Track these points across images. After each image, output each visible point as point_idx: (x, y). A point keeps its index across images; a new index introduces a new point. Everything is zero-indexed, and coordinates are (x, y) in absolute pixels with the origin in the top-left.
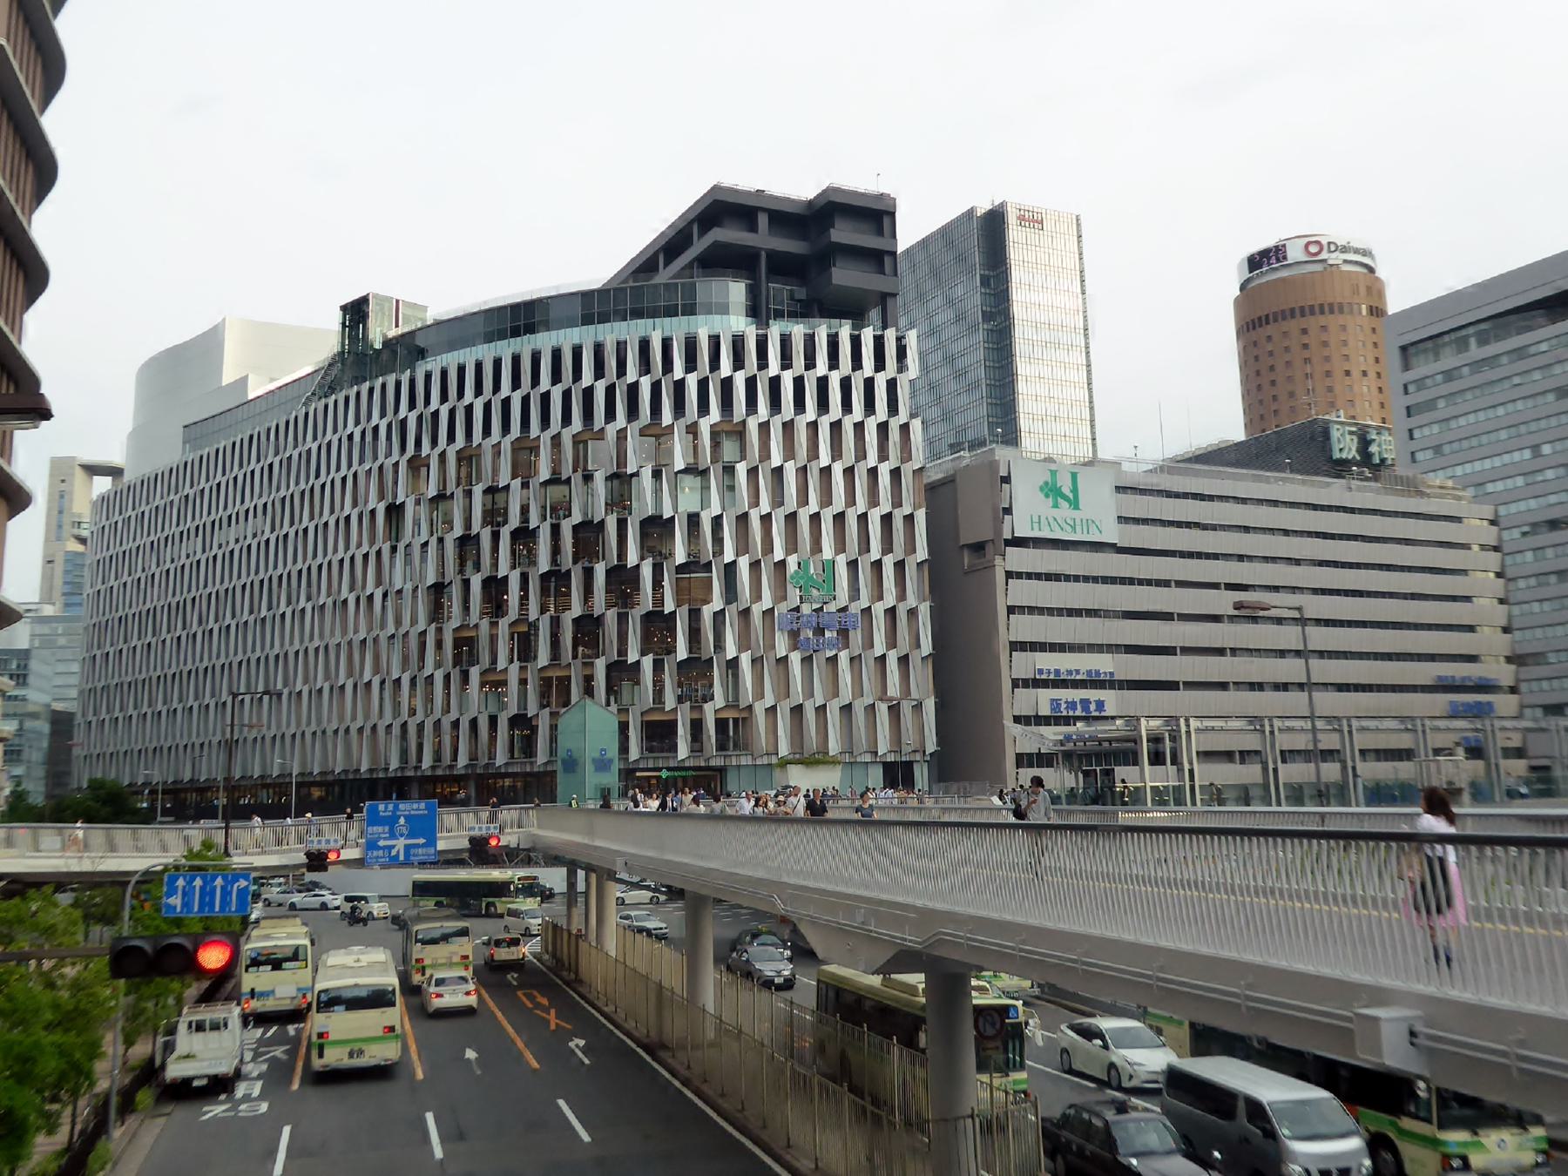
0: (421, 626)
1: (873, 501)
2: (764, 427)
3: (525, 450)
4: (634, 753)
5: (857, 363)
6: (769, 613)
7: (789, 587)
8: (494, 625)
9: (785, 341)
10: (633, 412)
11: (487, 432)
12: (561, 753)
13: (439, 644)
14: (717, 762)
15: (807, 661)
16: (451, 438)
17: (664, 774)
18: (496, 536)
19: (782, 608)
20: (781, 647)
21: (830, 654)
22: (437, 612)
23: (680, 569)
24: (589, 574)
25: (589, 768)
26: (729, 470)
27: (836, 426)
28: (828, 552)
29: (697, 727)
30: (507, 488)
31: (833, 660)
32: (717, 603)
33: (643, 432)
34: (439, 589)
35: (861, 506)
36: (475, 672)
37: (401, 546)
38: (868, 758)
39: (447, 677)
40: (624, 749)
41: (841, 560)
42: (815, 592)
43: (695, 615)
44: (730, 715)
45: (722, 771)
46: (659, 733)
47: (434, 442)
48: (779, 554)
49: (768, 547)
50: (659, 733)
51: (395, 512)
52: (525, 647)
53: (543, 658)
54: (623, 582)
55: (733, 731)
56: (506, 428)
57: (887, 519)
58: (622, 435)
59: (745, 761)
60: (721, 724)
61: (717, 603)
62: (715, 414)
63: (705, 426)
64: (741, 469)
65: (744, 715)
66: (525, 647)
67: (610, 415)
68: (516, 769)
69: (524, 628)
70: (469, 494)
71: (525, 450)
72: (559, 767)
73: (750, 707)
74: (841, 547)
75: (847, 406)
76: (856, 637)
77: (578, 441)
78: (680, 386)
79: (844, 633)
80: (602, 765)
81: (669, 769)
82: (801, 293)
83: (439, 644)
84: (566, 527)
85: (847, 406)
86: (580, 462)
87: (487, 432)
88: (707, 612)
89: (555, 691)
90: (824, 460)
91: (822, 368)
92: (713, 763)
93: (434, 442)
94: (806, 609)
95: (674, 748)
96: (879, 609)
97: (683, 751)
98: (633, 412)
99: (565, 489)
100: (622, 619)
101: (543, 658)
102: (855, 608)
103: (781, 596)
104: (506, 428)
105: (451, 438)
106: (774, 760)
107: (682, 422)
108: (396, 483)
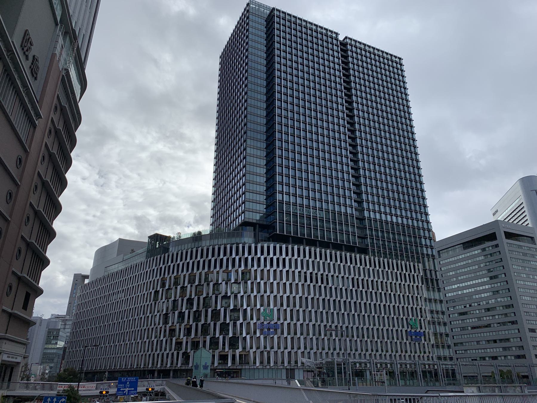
0: (161, 325)
1: (285, 292)
5: (281, 254)
8: (180, 325)
9: (262, 248)
10: (221, 266)
11: (182, 271)
12: (195, 364)
13: (165, 331)
15: (265, 338)
16: (173, 273)
17: (224, 371)
18: (183, 300)
19: (259, 322)
21: (271, 336)
22: (166, 322)
23: (231, 310)
24: (207, 311)
26: (246, 283)
27: (275, 271)
28: (272, 306)
29: (234, 357)
30: (187, 286)
32: (241, 320)
33: (223, 272)
34: (166, 315)
36: (174, 339)
37: (157, 302)
39: (166, 341)
40: (213, 363)
41: (275, 309)
42: (268, 318)
44: (243, 353)
45: (241, 369)
46: (223, 358)
47: (169, 274)
48: (258, 307)
49: (255, 305)
50: (223, 358)
51: (157, 292)
52: (188, 331)
53: (193, 335)
54: (216, 314)
55: (244, 359)
56: (188, 270)
58: (218, 273)
59: (247, 367)
60: (240, 355)
61: (241, 320)
62: (243, 267)
63: (240, 270)
65: (247, 353)
66: (188, 331)
67: (215, 267)
68: (184, 368)
69: (189, 327)
70: (176, 288)
72: (193, 368)
75: (278, 266)
76: (279, 331)
77: (206, 274)
78: (234, 259)
79: (276, 330)
80: (205, 367)
81: (226, 369)
82: (267, 235)
83: (165, 331)
84: (201, 298)
85: (278, 266)
86: (206, 279)
87: (182, 271)
88: (238, 323)
89: (195, 345)
90: (271, 281)
92: (238, 368)
93: (169, 274)
94: (265, 323)
96: (286, 323)
97: (230, 364)
98: (221, 266)
99: (201, 287)
101: (193, 335)
102: (279, 323)
103: (258, 319)
104: (188, 270)
105: (173, 273)
107: (234, 269)
108: (157, 285)
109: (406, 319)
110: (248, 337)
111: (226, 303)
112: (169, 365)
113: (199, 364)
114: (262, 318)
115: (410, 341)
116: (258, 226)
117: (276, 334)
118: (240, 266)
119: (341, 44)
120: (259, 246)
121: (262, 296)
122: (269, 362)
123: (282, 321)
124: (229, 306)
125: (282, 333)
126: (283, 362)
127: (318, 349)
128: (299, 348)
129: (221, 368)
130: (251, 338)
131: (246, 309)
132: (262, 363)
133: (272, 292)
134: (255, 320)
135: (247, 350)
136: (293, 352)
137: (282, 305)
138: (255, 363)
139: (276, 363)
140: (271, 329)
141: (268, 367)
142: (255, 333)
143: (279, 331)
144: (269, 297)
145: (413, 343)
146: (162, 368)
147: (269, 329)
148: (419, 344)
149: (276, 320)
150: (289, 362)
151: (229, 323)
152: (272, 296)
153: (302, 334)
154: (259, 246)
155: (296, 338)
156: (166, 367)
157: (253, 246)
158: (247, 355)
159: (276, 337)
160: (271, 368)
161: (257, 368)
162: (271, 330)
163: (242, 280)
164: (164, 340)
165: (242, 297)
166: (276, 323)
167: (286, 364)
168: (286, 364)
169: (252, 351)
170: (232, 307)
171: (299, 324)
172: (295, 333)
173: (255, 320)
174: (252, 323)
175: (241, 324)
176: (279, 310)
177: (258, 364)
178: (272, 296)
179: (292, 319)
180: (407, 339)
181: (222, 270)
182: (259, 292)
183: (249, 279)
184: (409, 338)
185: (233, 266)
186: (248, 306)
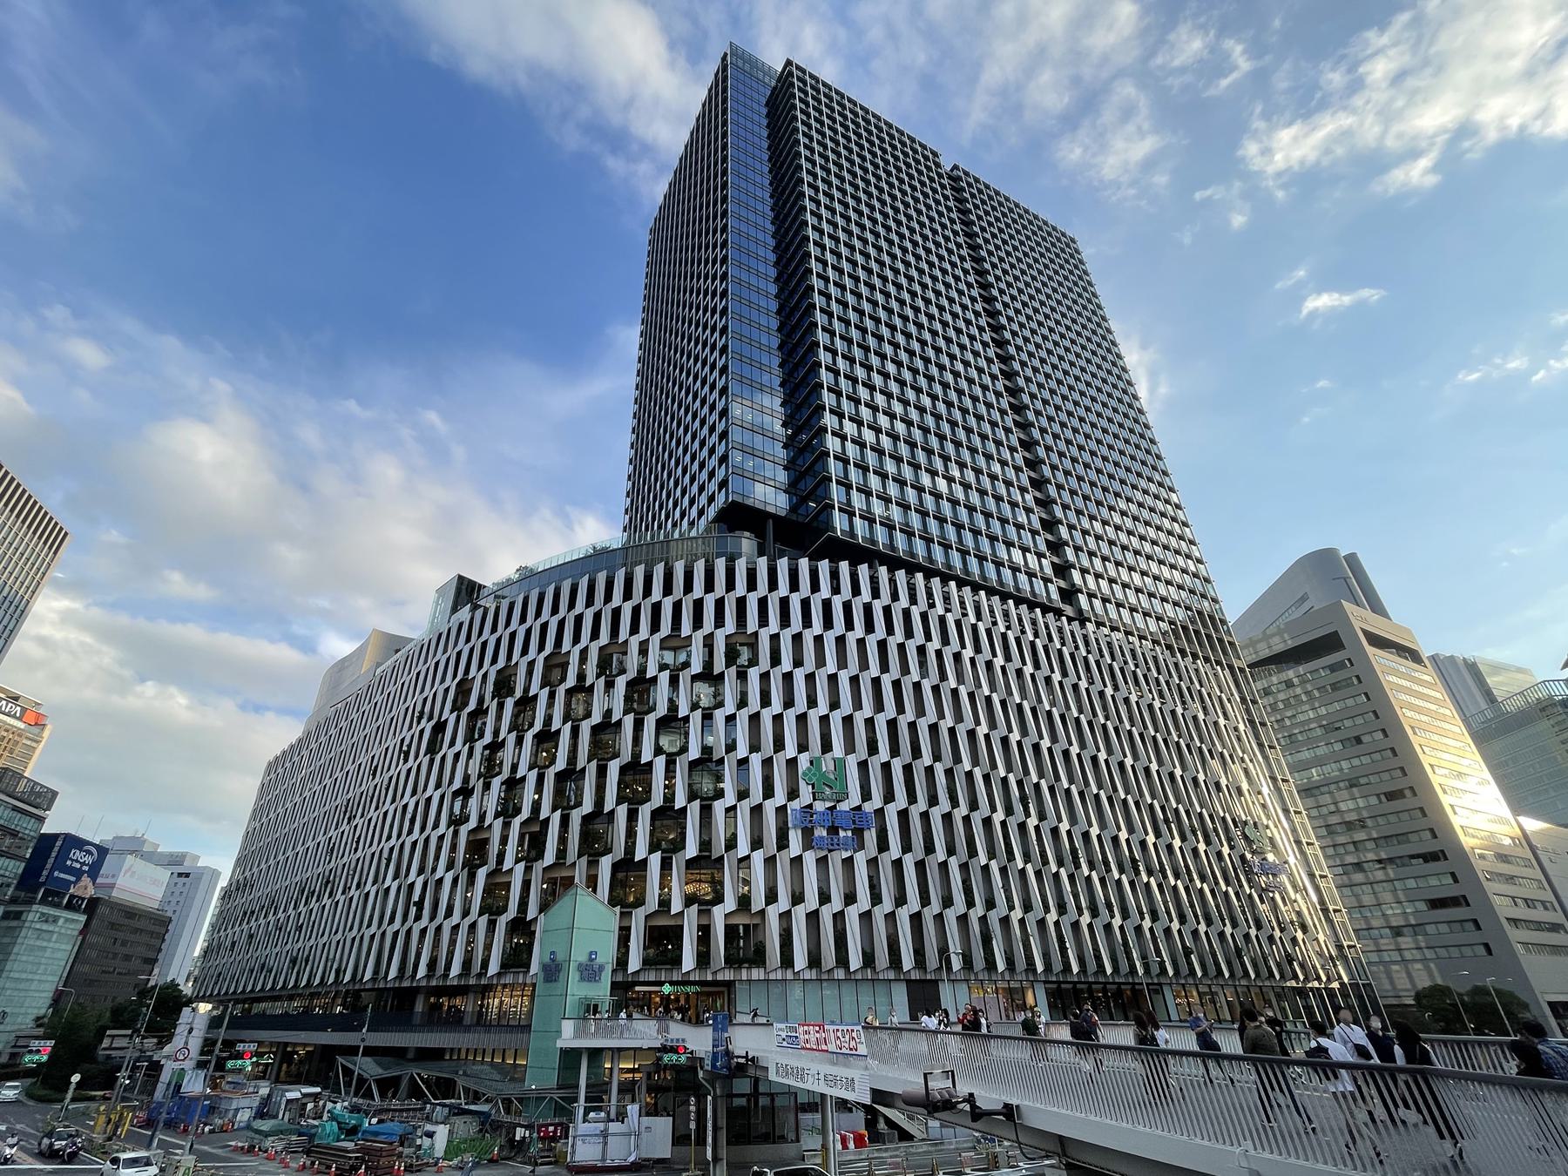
1: (879, 706)
4: (634, 964)
6: (781, 810)
7: (802, 784)
13: (454, 848)
14: (727, 975)
15: (822, 862)
20: (795, 847)
21: (846, 855)
25: (574, 976)
27: (841, 640)
28: (838, 749)
29: (705, 933)
31: (848, 862)
32: (730, 799)
36: (482, 873)
41: (852, 762)
42: (828, 791)
43: (706, 811)
44: (741, 920)
45: (729, 985)
46: (663, 940)
50: (663, 940)
52: (534, 843)
59: (757, 974)
60: (731, 931)
66: (534, 843)
74: (850, 748)
76: (871, 837)
79: (859, 832)
80: (590, 972)
83: (454, 848)
92: (720, 977)
94: (820, 806)
95: (678, 962)
97: (688, 961)
100: (632, 816)
102: (869, 807)
103: (793, 794)
106: (790, 976)
112: (455, 970)
113: (560, 957)
114: (806, 792)
121: (802, 719)
123: (877, 801)
125: (883, 845)
129: (652, 978)
134: (780, 798)
141: (840, 974)
142: (783, 843)
143: (871, 837)
146: (434, 983)
147: (833, 830)
149: (855, 799)
151: (685, 808)
152: (836, 719)
153: (951, 851)
156: (446, 976)
159: (860, 859)
162: (842, 834)
164: (449, 877)
165: (730, 719)
166: (859, 808)
169: (773, 912)
170: (694, 753)
173: (780, 798)
174: (770, 807)
182: (789, 703)
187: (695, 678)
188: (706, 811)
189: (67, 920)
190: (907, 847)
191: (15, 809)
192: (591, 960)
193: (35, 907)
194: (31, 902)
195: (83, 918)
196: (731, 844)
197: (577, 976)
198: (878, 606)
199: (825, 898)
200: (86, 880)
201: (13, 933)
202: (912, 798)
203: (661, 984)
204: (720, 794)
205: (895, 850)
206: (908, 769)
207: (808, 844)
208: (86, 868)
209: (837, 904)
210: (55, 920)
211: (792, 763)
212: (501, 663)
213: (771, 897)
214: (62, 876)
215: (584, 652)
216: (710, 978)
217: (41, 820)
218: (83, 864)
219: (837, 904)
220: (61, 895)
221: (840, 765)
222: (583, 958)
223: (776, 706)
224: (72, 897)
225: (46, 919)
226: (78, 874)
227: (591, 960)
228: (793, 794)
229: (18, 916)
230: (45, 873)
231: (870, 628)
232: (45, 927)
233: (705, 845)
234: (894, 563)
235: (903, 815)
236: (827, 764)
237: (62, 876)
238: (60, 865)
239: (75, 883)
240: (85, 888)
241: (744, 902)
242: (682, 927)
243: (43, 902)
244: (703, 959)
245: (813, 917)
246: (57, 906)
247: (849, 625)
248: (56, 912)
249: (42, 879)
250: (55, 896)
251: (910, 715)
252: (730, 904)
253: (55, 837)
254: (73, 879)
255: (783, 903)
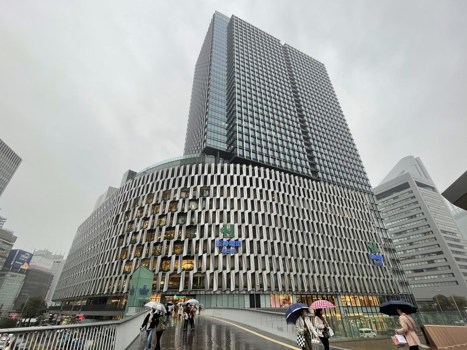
1: (246, 208)
2: (215, 188)
3: (150, 196)
11: (142, 193)
14: (193, 293)
15: (224, 257)
20: (216, 253)
21: (232, 255)
26: (204, 199)
27: (235, 188)
28: (232, 222)
29: (187, 279)
31: (233, 257)
35: (242, 210)
38: (244, 292)
39: (117, 263)
41: (236, 226)
42: (228, 235)
43: (190, 242)
44: (199, 275)
48: (217, 222)
57: (250, 214)
60: (195, 279)
61: (198, 238)
63: (199, 187)
64: (208, 199)
71: (150, 196)
73: (205, 273)
74: (236, 221)
76: (241, 249)
79: (237, 248)
88: (194, 240)
91: (232, 173)
92: (191, 293)
94: (225, 240)
96: (248, 241)
97: (181, 289)
102: (240, 240)
103: (217, 236)
106: (212, 293)
109: (365, 242)
110: (205, 256)
111: (182, 221)
114: (221, 235)
115: (373, 265)
116: (218, 152)
117: (237, 252)
118: (199, 183)
119: (283, 47)
120: (219, 166)
121: (222, 213)
122: (229, 286)
123: (243, 238)
124: (185, 223)
125: (244, 252)
126: (246, 286)
127: (285, 270)
128: (264, 269)
130: (208, 257)
131: (204, 225)
132: (220, 287)
133: (232, 208)
134: (213, 237)
135: (203, 272)
136: (257, 273)
137: (243, 221)
138: (212, 287)
139: (237, 287)
140: (230, 247)
142: (213, 251)
143: (241, 249)
144: (229, 213)
145: (375, 267)
147: (229, 247)
148: (381, 267)
149: (236, 237)
150: (253, 286)
151: (184, 241)
152: (232, 212)
153: (266, 253)
154: (219, 166)
155: (260, 257)
157: (213, 165)
158: (203, 278)
159: (237, 256)
160: (231, 293)
161: (215, 293)
162: (231, 248)
163: (200, 197)
166: (237, 240)
167: (249, 288)
168: (249, 288)
169: (208, 273)
171: (262, 241)
172: (259, 252)
173: (213, 237)
174: (210, 240)
175: (198, 242)
176: (240, 227)
177: (215, 288)
178: (232, 212)
179: (255, 236)
180: (370, 263)
181: (180, 188)
182: (218, 208)
183: (208, 196)
184: (371, 261)
185: (192, 184)
186: (206, 222)
187: (190, 200)
188: (190, 242)
189: (20, 276)
190: (252, 252)
191: (3, 242)
192: (145, 288)
193: (9, 272)
194: (8, 271)
195: (25, 276)
196: (197, 252)
197: (139, 293)
198: (260, 179)
199: (224, 268)
200: (26, 264)
201: (2, 280)
202: (255, 236)
203: (173, 295)
204: (195, 236)
205: (248, 253)
206: (254, 228)
207: (220, 252)
208: (26, 260)
209: (244, 270)
210: (16, 276)
211: (218, 226)
212: (136, 197)
213: (208, 269)
214: (18, 263)
215: (159, 193)
216: (188, 294)
217: (12, 245)
218: (25, 259)
219: (228, 270)
220: (18, 269)
221: (232, 227)
222: (142, 287)
223: (214, 209)
224: (21, 269)
225: (12, 276)
226: (23, 262)
227: (145, 288)
228: (217, 236)
229: (4, 275)
230: (13, 262)
231: (257, 186)
232: (12, 278)
233: (189, 252)
234: (260, 165)
235: (251, 242)
236: (228, 227)
237: (18, 263)
238: (17, 259)
239: (22, 265)
240: (25, 267)
241: (199, 269)
242: (180, 278)
243: (12, 271)
244: (186, 287)
245: (220, 274)
246: (17, 272)
247: (251, 185)
248: (16, 274)
249: (12, 264)
250: (16, 269)
251: (256, 211)
252: (195, 271)
253: (16, 250)
254: (21, 264)
255: (211, 270)
